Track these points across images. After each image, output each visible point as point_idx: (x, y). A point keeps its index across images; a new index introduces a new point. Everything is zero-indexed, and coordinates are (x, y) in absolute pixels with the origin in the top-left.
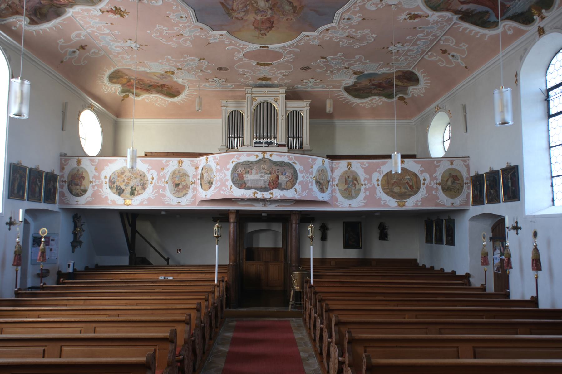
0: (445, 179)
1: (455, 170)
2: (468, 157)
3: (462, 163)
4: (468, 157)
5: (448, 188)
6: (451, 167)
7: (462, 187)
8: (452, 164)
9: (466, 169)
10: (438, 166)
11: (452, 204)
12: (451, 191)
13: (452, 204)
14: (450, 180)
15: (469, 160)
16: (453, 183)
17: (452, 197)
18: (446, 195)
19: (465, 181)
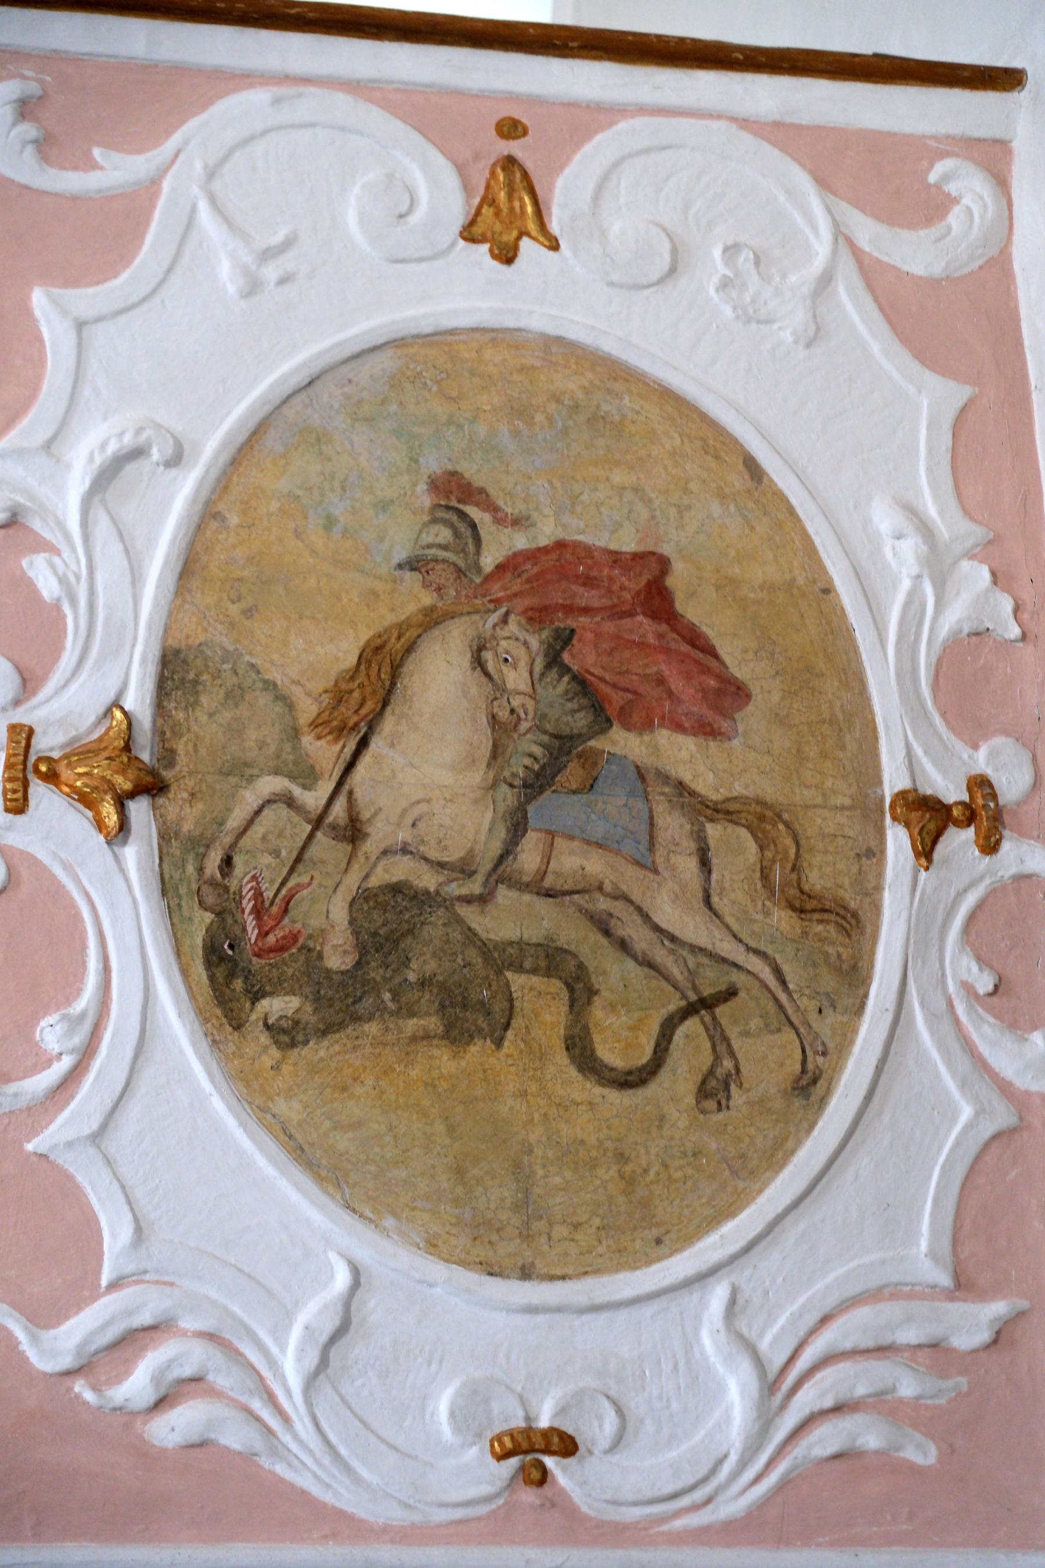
0: (314, 655)
1: (599, 398)
2: (1003, 79)
3: (811, 222)
4: (1003, 79)
5: (391, 917)
6: (470, 292)
7: (841, 921)
8: (507, 213)
9: (930, 401)
10: (109, 233)
11: (534, 1451)
12: (470, 1012)
13: (534, 1451)
14: (441, 676)
15: (993, 157)
16: (544, 769)
17: (510, 1225)
18: (301, 1151)
19: (911, 751)
